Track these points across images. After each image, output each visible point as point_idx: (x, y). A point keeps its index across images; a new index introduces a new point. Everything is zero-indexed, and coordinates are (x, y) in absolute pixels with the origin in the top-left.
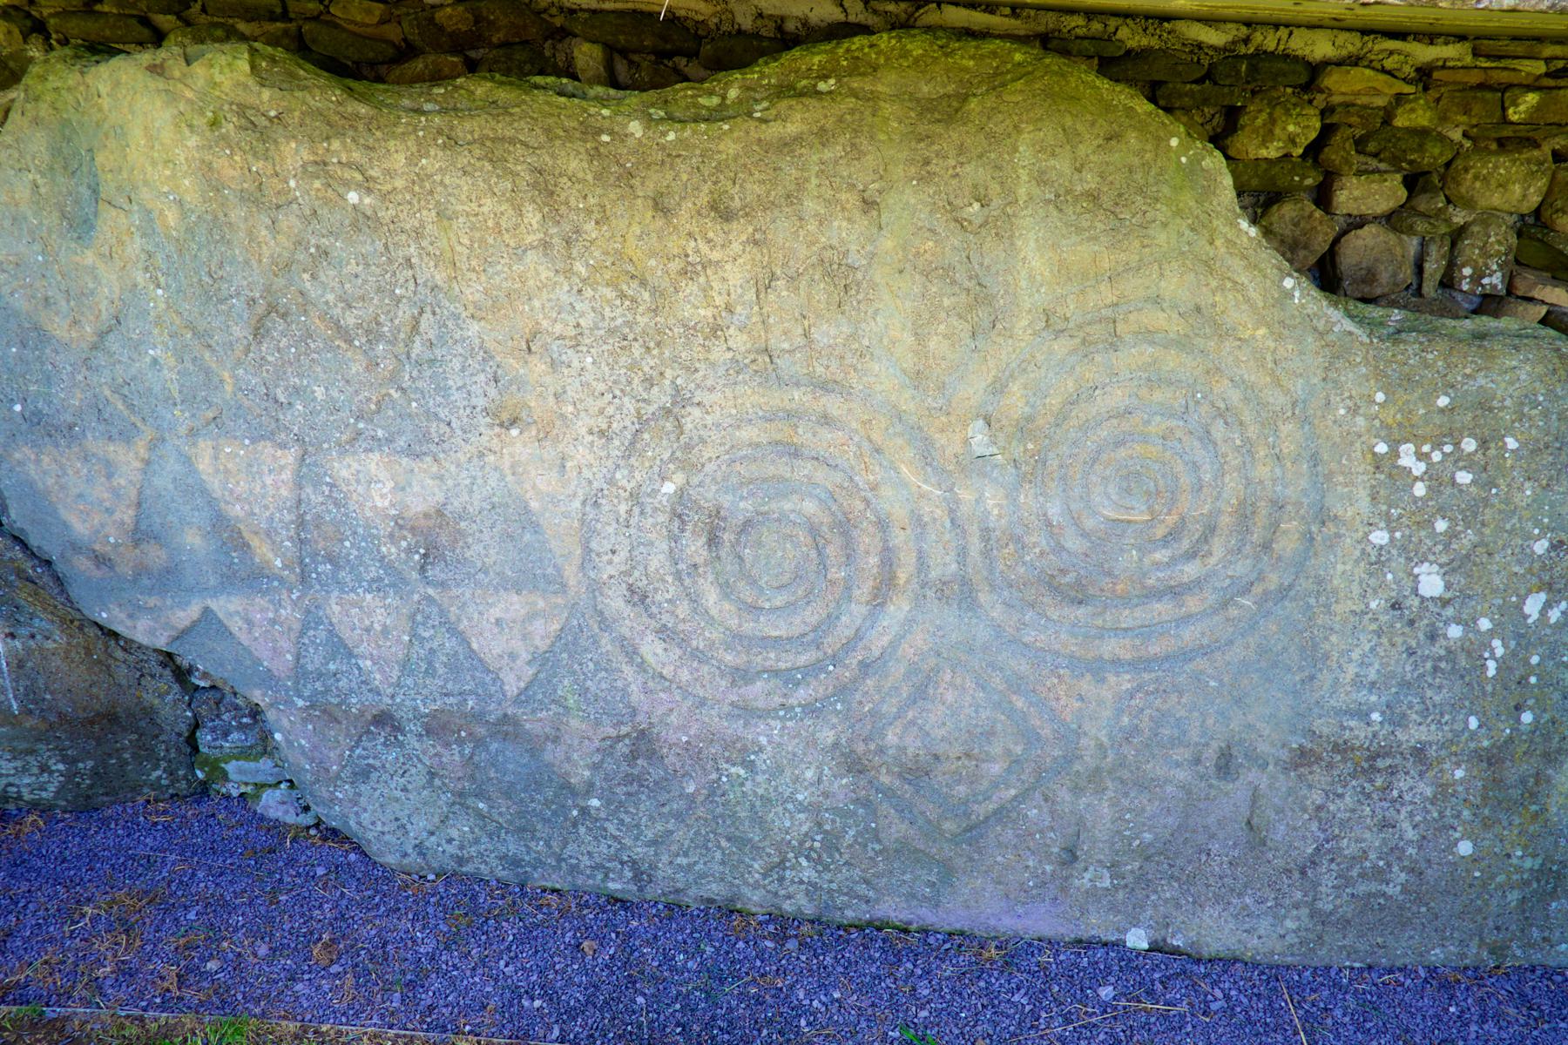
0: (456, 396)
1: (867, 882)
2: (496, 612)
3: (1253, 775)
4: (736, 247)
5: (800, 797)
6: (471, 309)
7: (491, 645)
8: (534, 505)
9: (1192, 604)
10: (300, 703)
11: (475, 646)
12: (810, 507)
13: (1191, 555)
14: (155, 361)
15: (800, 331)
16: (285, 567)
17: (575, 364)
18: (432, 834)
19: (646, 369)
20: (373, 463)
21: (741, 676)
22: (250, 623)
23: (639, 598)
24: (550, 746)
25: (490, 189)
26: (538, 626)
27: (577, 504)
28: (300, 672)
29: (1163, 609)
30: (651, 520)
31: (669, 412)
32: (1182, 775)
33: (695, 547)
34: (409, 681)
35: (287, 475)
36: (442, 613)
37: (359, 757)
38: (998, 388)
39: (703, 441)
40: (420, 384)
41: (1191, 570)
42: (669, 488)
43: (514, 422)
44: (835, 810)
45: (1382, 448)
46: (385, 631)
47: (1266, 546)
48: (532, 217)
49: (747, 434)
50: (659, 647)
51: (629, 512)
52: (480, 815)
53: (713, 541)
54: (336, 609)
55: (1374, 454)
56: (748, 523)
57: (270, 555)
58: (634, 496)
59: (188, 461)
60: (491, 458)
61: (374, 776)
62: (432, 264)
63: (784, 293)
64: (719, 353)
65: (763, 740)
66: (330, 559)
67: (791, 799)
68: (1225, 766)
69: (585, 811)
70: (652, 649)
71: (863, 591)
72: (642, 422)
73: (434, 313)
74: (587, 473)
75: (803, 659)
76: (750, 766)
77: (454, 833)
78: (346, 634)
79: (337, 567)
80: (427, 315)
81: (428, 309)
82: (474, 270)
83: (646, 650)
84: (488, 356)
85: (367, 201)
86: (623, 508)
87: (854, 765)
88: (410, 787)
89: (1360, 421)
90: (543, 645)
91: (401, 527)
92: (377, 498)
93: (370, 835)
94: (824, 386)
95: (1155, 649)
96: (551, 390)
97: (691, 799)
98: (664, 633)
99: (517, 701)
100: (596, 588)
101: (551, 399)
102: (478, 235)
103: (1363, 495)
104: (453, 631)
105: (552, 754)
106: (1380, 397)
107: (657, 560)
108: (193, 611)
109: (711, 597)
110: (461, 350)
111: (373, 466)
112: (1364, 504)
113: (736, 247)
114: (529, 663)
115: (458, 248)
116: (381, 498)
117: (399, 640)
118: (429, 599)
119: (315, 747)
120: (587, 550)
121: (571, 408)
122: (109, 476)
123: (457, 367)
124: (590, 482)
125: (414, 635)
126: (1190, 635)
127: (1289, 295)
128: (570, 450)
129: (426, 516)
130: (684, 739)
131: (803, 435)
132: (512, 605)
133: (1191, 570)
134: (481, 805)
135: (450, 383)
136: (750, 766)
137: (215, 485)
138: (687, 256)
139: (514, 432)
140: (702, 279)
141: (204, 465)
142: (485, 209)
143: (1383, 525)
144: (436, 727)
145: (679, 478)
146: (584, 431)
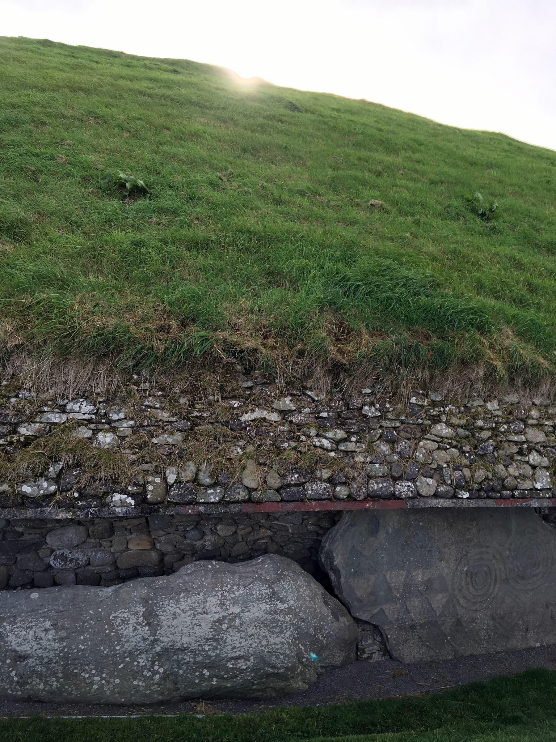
0: (434, 556)
1: (495, 644)
2: (437, 598)
3: (551, 607)
7: (434, 606)
10: (395, 627)
12: (485, 569)
13: (537, 569)
14: (383, 557)
16: (400, 596)
20: (420, 572)
21: (475, 603)
22: (390, 610)
23: (460, 591)
28: (397, 619)
29: (535, 579)
32: (541, 609)
33: (469, 579)
34: (419, 617)
35: (404, 576)
36: (428, 600)
38: (511, 544)
41: (538, 571)
42: (466, 569)
43: (442, 561)
44: (490, 629)
46: (418, 606)
47: (547, 566)
49: (477, 557)
52: (428, 646)
53: (471, 578)
56: (476, 574)
57: (396, 594)
59: (385, 576)
64: (473, 544)
66: (408, 592)
67: (483, 629)
68: (547, 607)
69: (447, 640)
70: (462, 601)
71: (492, 584)
72: (462, 557)
75: (484, 598)
76: (476, 623)
77: (421, 652)
78: (409, 608)
79: (409, 593)
84: (439, 548)
87: (493, 618)
93: (405, 657)
94: (488, 547)
95: (534, 587)
97: (466, 632)
98: (464, 597)
99: (438, 617)
100: (453, 590)
105: (443, 628)
107: (463, 583)
108: (378, 609)
109: (471, 589)
116: (420, 578)
118: (426, 598)
119: (397, 637)
120: (453, 583)
122: (368, 582)
125: (422, 606)
129: (427, 580)
132: (440, 596)
133: (538, 571)
136: (476, 623)
137: (389, 580)
141: (388, 577)
144: (422, 626)
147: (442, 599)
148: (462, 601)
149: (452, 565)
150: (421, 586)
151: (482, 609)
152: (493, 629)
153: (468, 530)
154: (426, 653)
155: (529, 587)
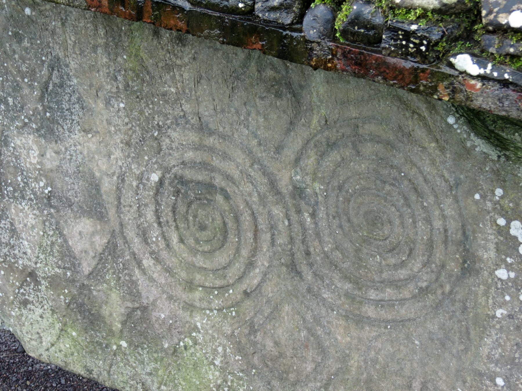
4: (186, 60)
5: (217, 362)
6: (73, 71)
7: (77, 245)
8: (97, 174)
9: (406, 294)
11: (70, 243)
13: (403, 264)
15: (212, 107)
17: (116, 106)
18: (53, 345)
19: (147, 114)
21: (190, 286)
24: (104, 307)
25: (85, 15)
26: (97, 238)
27: (115, 178)
29: (389, 293)
30: (147, 192)
31: (156, 139)
37: (23, 294)
39: (170, 154)
40: (53, 105)
45: (502, 222)
46: (33, 227)
48: (102, 32)
49: (190, 155)
50: (151, 262)
51: (138, 187)
54: (13, 211)
55: (498, 225)
58: (140, 178)
60: (79, 147)
61: (29, 306)
62: (58, 47)
63: (205, 87)
65: (199, 325)
67: (214, 365)
69: (119, 347)
70: (147, 262)
73: (58, 71)
74: (120, 163)
80: (55, 72)
81: (56, 69)
82: (75, 53)
83: (145, 262)
85: (34, 13)
86: (135, 184)
88: (44, 316)
89: (489, 204)
90: (100, 250)
91: (41, 175)
92: (32, 158)
93: (26, 339)
96: (105, 117)
99: (88, 277)
101: (105, 122)
102: (78, 37)
103: (492, 246)
104: (61, 235)
106: (499, 192)
107: (150, 215)
110: (69, 91)
111: (30, 142)
112: (492, 254)
113: (186, 60)
114: (94, 258)
115: (69, 42)
117: (38, 233)
121: (113, 129)
123: (67, 98)
124: (121, 168)
126: (403, 312)
127: (450, 126)
128: (113, 150)
130: (163, 316)
131: (216, 162)
133: (402, 273)
134: (74, 334)
135: (64, 106)
138: (166, 60)
139: (90, 136)
140: (171, 74)
142: (81, 25)
143: (503, 266)
145: (159, 173)
146: (119, 141)
147: (93, 234)
148: (147, 262)
149: (117, 154)
150: (37, 180)
151: (211, 310)
152: (240, 379)
153: (169, 68)
154: (72, 354)
155: (370, 311)
